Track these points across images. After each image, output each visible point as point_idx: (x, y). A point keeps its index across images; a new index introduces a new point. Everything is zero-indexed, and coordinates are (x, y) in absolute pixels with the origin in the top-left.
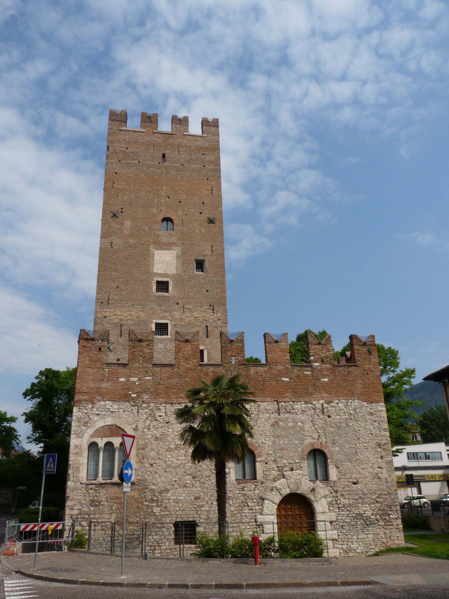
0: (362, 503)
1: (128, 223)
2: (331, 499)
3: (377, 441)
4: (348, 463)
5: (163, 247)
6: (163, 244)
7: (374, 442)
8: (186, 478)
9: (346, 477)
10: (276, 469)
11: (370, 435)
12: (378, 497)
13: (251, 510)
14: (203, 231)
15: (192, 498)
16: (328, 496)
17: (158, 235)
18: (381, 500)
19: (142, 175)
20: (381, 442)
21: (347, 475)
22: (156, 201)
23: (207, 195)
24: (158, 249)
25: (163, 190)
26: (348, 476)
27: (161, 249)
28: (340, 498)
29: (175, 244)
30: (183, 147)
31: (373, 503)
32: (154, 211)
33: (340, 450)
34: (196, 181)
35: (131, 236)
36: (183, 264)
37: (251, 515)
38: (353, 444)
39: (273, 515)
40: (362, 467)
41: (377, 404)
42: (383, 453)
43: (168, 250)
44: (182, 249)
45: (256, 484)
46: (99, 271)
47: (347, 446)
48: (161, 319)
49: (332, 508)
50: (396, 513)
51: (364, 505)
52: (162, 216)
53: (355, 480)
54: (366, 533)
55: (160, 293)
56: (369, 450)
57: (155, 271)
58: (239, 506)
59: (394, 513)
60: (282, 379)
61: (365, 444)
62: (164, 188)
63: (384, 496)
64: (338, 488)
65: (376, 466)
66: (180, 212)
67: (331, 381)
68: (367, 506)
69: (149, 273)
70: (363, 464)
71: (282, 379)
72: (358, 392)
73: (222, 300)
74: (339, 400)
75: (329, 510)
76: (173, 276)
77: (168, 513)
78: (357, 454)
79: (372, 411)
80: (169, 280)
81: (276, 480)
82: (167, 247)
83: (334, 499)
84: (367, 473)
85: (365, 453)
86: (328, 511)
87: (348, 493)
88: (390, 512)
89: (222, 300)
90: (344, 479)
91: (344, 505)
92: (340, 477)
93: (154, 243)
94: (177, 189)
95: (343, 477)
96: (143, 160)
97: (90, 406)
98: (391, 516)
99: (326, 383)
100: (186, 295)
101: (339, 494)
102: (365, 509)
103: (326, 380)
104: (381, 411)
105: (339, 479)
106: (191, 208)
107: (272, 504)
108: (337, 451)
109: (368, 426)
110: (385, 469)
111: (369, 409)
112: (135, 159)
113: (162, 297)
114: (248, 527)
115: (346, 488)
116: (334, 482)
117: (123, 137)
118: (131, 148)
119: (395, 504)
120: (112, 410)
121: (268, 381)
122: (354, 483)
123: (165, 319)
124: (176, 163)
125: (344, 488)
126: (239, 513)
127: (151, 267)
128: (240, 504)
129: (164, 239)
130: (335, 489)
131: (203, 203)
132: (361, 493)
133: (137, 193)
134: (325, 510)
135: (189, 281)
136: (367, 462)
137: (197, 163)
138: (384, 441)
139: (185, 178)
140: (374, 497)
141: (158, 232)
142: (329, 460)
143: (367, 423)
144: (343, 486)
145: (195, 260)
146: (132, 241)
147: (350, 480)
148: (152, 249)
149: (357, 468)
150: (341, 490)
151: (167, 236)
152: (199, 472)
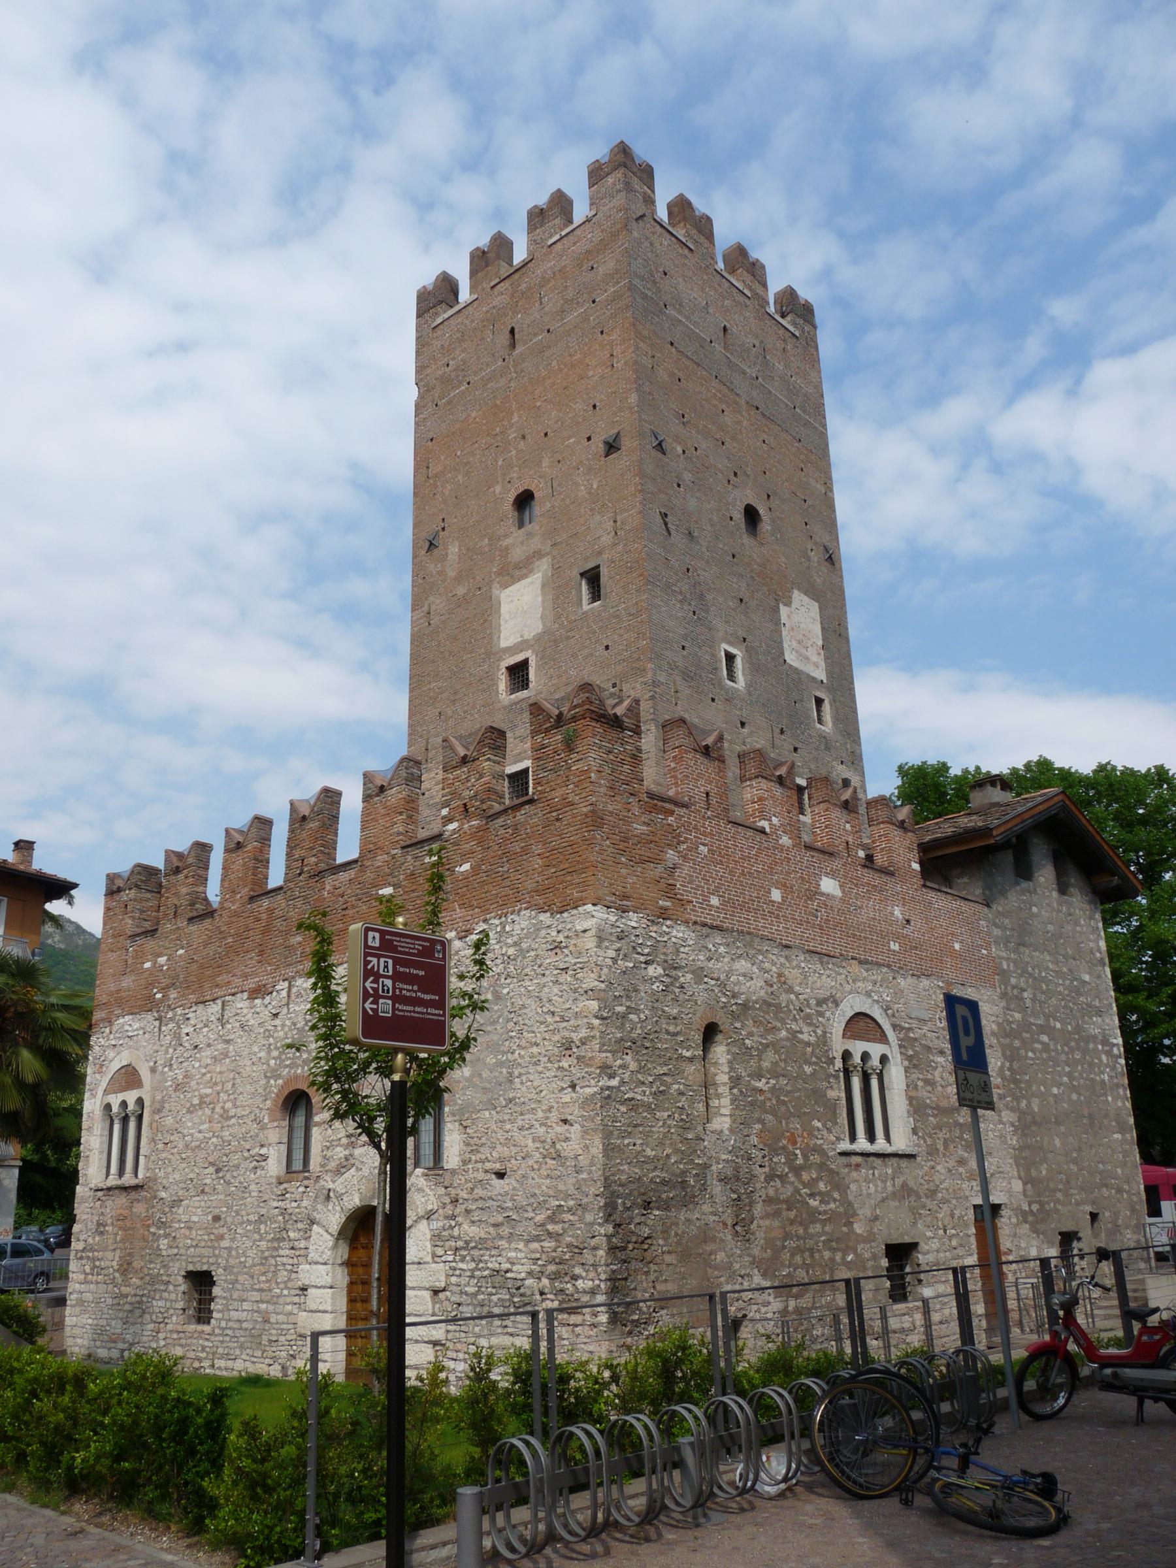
0: (510, 1238)
1: (454, 550)
2: (440, 1224)
3: (566, 1034)
4: (487, 1114)
5: (517, 572)
6: (517, 567)
7: (557, 1038)
8: (207, 1171)
9: (479, 1156)
10: (345, 1141)
11: (549, 1019)
12: (552, 1219)
13: (292, 1248)
14: (595, 486)
15: (210, 1218)
16: (436, 1216)
17: (507, 548)
18: (558, 1228)
19: (474, 414)
20: (574, 1035)
21: (482, 1149)
22: (500, 463)
23: (602, 377)
24: (506, 586)
25: (511, 427)
26: (485, 1153)
27: (515, 580)
28: (459, 1219)
29: (538, 554)
30: (549, 281)
31: (537, 1239)
32: (498, 489)
33: (472, 1076)
34: (578, 356)
35: (458, 579)
36: (556, 599)
37: (291, 1261)
38: (504, 1053)
39: (325, 1264)
40: (520, 1123)
41: (574, 912)
42: (577, 1073)
43: (525, 576)
44: (554, 558)
45: (306, 1182)
46: (411, 691)
47: (491, 1060)
48: (515, 763)
49: (440, 1251)
50: (592, 1275)
51: (513, 1245)
52: (511, 496)
53: (498, 1166)
54: (510, 1330)
55: (513, 696)
56: (540, 1069)
57: (504, 644)
58: (273, 1240)
59: (587, 1271)
60: (380, 892)
61: (535, 1050)
62: (515, 419)
63: (567, 1217)
64: (459, 1191)
65: (554, 1116)
66: (546, 463)
67: (475, 870)
68: (521, 1246)
69: (492, 654)
70: (522, 1114)
71: (380, 892)
72: (530, 885)
73: (639, 659)
74: (485, 921)
75: (434, 1255)
76: (538, 638)
77: (176, 1251)
78: (511, 1082)
79: (561, 938)
80: (528, 654)
81: (343, 1170)
82: (524, 571)
83: (447, 1223)
84: (530, 1142)
85: (531, 1077)
86: (429, 1259)
87: (480, 1204)
88: (578, 1270)
89: (639, 659)
90: (476, 1162)
91: (467, 1243)
92: (467, 1156)
93: (499, 574)
94: (538, 404)
95: (473, 1158)
96: (476, 373)
97: (107, 1030)
98: (580, 1283)
99: (466, 876)
100: (564, 679)
101: (460, 1209)
102: (513, 1254)
103: (466, 867)
104: (585, 931)
105: (464, 1162)
106: (570, 437)
107: (325, 1234)
108: (467, 1080)
109: (546, 990)
110: (577, 1126)
111: (554, 934)
112: (461, 382)
113: (516, 704)
114: (285, 1292)
115: (479, 1192)
116: (453, 1172)
117: (439, 343)
118: (454, 359)
119: (593, 1242)
120: (130, 1034)
121: (353, 907)
122: (501, 1175)
123: (521, 761)
124: (536, 335)
125: (472, 1189)
126: (273, 1257)
127: (495, 638)
128: (275, 1233)
129: (517, 554)
130: (453, 1191)
131: (594, 407)
132: (510, 1204)
133: (466, 464)
134: (421, 1254)
135: (568, 638)
136: (533, 1106)
137: (578, 303)
138: (583, 1033)
139: (554, 363)
140: (540, 1218)
141: (505, 543)
142: (447, 1109)
143: (544, 980)
144: (470, 1185)
145: (582, 575)
146: (461, 591)
147: (488, 1166)
148: (495, 592)
149: (508, 1127)
150: (466, 1196)
151: (522, 543)
152: (225, 1159)
